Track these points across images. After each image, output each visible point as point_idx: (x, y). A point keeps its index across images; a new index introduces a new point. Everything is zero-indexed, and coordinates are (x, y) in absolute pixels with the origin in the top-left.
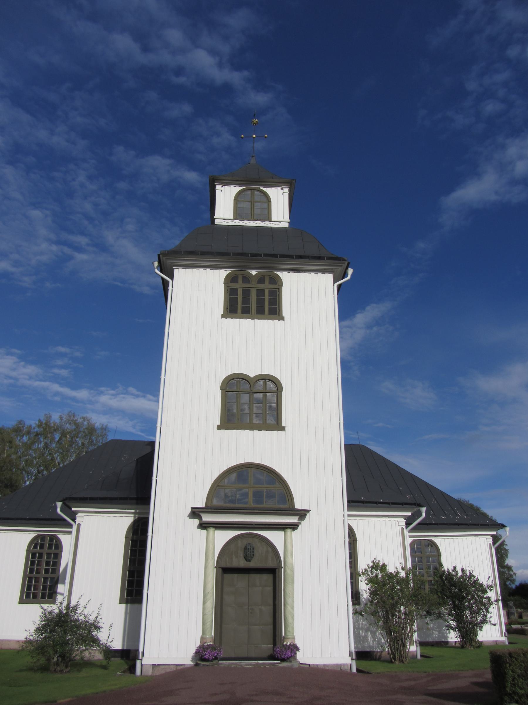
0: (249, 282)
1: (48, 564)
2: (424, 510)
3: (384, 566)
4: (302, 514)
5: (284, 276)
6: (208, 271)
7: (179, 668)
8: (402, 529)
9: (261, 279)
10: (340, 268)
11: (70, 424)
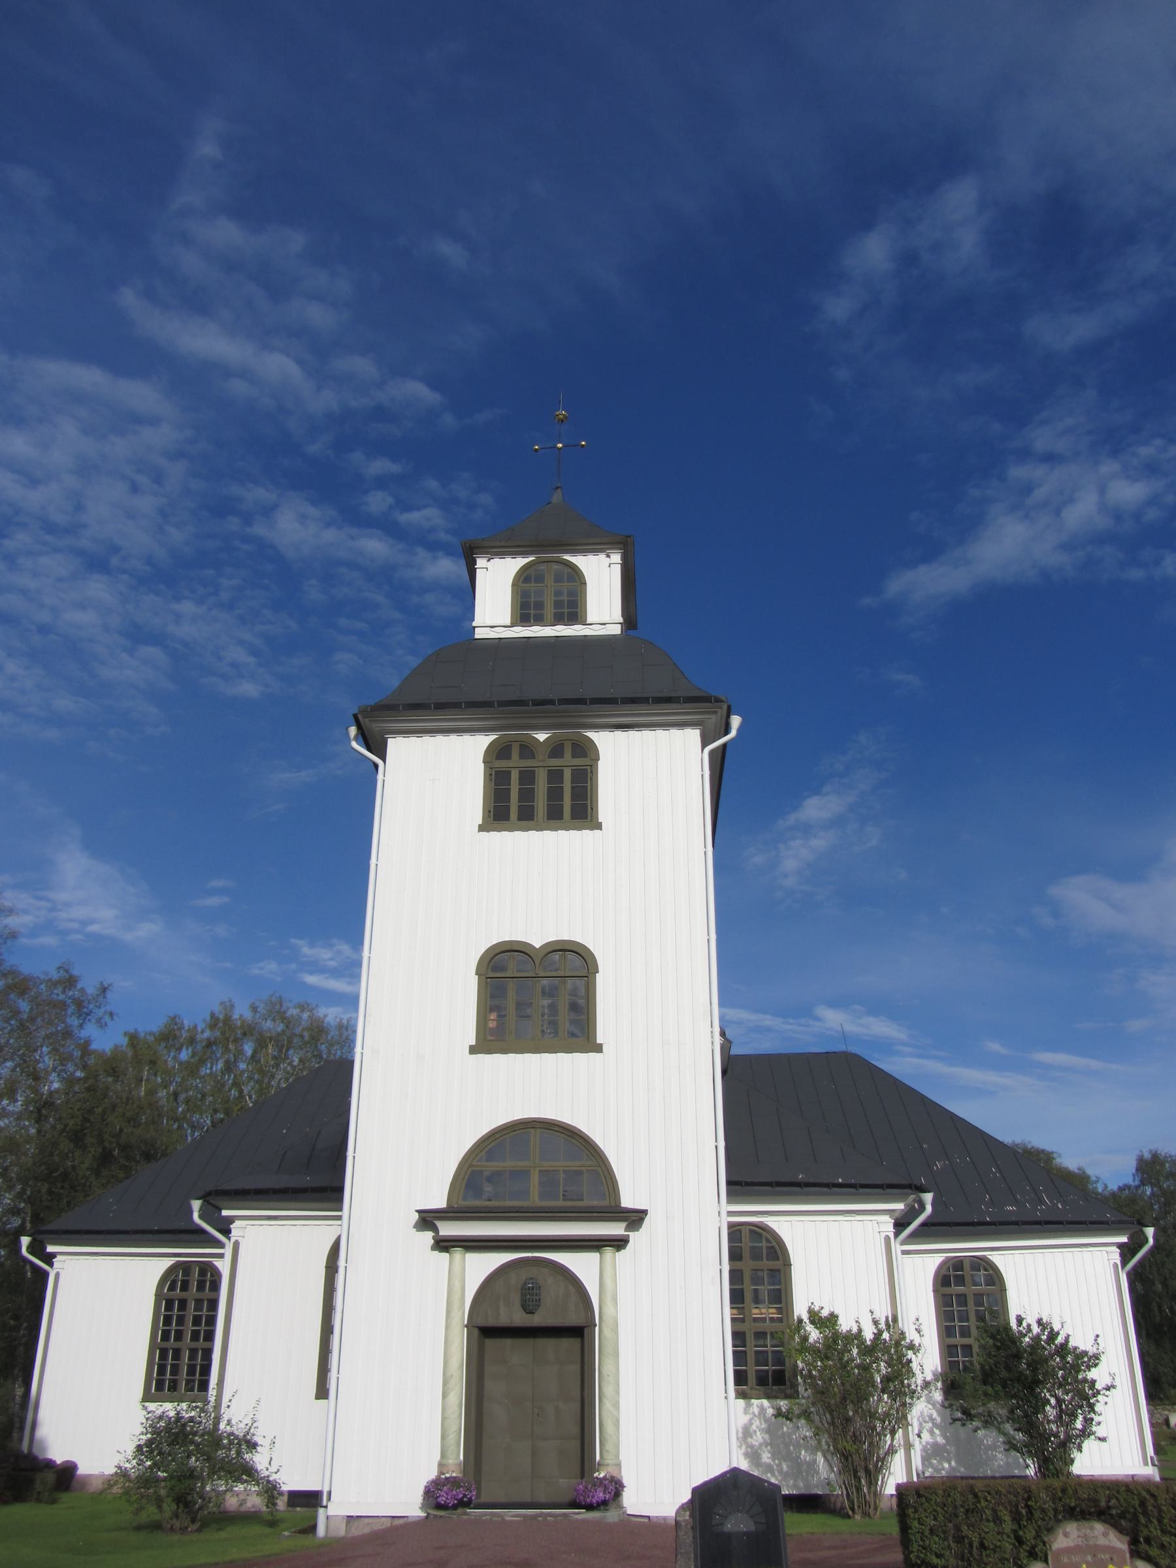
0: (532, 756)
1: (197, 1320)
2: (928, 1197)
3: (833, 1318)
4: (635, 1218)
5: (601, 738)
6: (453, 738)
7: (397, 1522)
8: (887, 1238)
9: (556, 749)
10: (713, 717)
11: (274, 1020)
